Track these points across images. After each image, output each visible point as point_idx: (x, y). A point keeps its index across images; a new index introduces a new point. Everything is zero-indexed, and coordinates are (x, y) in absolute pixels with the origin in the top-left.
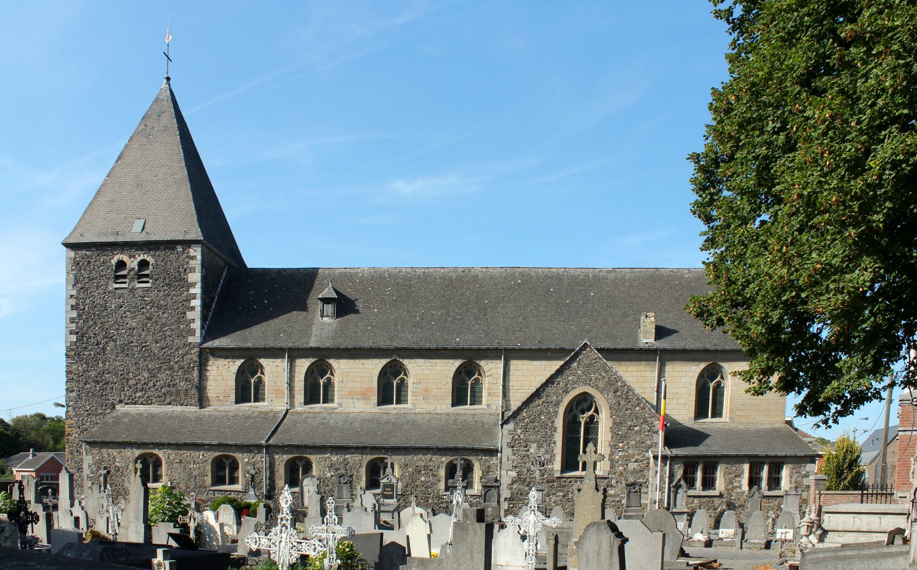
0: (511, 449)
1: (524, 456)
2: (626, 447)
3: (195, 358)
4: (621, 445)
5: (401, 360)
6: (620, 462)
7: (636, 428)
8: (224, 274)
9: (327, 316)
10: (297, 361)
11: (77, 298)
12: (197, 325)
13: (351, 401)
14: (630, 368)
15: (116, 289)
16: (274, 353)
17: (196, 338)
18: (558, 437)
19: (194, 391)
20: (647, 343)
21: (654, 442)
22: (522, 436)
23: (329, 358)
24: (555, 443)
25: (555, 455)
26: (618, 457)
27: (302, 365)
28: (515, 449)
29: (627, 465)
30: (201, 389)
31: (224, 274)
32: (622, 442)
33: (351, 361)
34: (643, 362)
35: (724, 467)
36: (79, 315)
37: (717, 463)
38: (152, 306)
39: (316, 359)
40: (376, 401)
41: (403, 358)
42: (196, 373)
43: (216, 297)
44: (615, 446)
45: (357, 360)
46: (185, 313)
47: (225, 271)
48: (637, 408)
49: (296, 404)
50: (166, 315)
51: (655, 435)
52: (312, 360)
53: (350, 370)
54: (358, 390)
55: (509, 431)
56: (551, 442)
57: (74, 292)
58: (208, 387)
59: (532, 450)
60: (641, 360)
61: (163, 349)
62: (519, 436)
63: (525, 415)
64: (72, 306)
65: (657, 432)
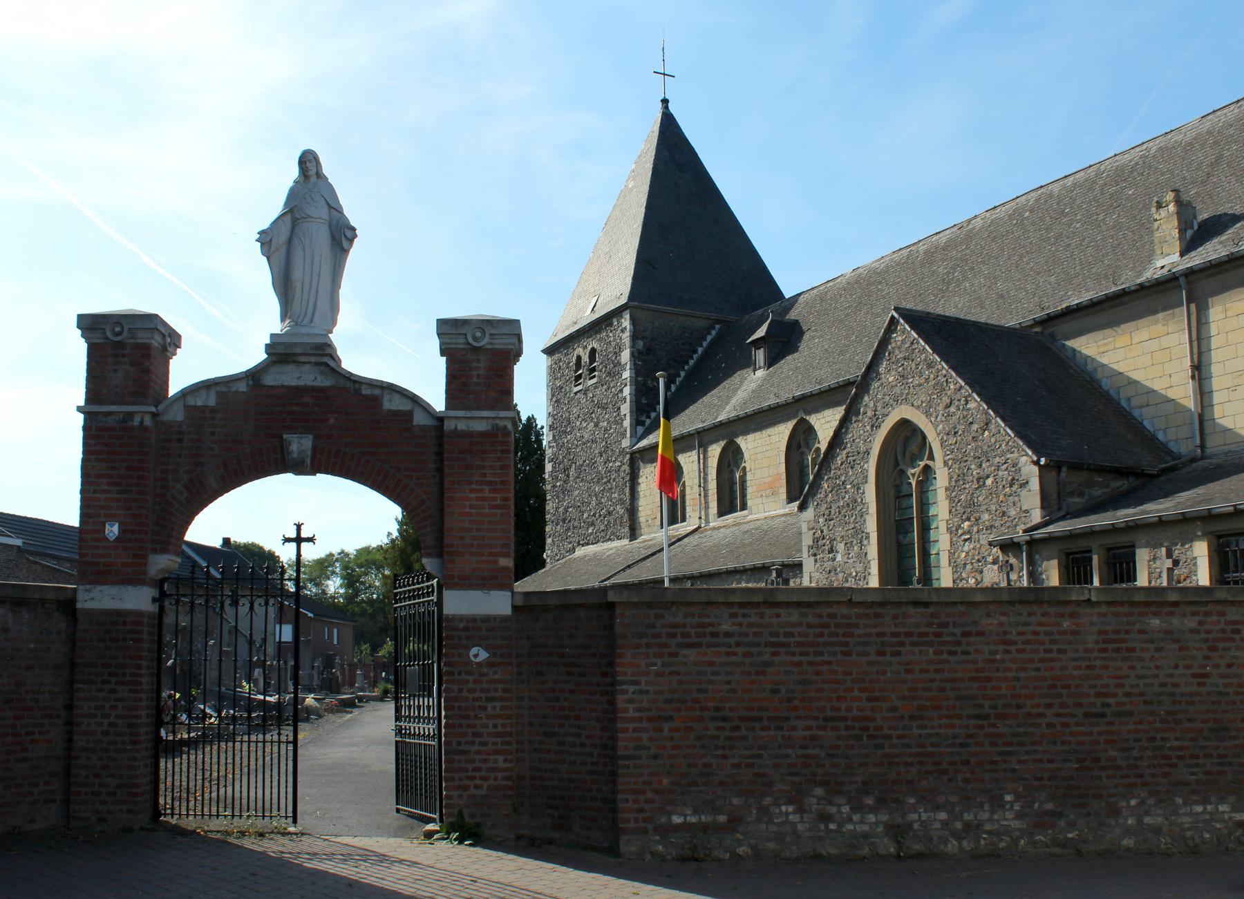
0: (812, 558)
1: (830, 572)
2: (975, 529)
3: (626, 468)
4: (967, 524)
5: (808, 418)
6: (969, 567)
7: (989, 482)
8: (709, 338)
9: (760, 368)
10: (709, 449)
11: (553, 416)
12: (627, 423)
13: (760, 500)
14: (1137, 337)
15: (576, 393)
16: (682, 443)
17: (626, 443)
18: (871, 525)
19: (626, 517)
20: (1162, 267)
21: (1024, 508)
22: (825, 529)
23: (737, 436)
24: (868, 538)
25: (869, 562)
26: (964, 554)
27: (715, 451)
28: (818, 557)
29: (981, 572)
30: (633, 511)
31: (709, 338)
32: (968, 519)
33: (758, 434)
34: (1160, 316)
35: (1147, 558)
36: (554, 436)
37: (1133, 546)
38: (598, 407)
39: (725, 442)
40: (784, 496)
41: (809, 413)
42: (627, 490)
43: (683, 374)
44: (957, 530)
45: (764, 432)
46: (619, 409)
47: (714, 332)
48: (986, 433)
49: (711, 518)
50: (607, 416)
51: (1023, 493)
52: (722, 443)
53: (758, 450)
54: (767, 480)
55: (809, 522)
56: (860, 534)
57: (551, 409)
58: (640, 509)
59: (839, 558)
60: (1155, 312)
61: (605, 463)
62: (822, 532)
63: (826, 485)
64: (550, 426)
65: (1025, 484)
